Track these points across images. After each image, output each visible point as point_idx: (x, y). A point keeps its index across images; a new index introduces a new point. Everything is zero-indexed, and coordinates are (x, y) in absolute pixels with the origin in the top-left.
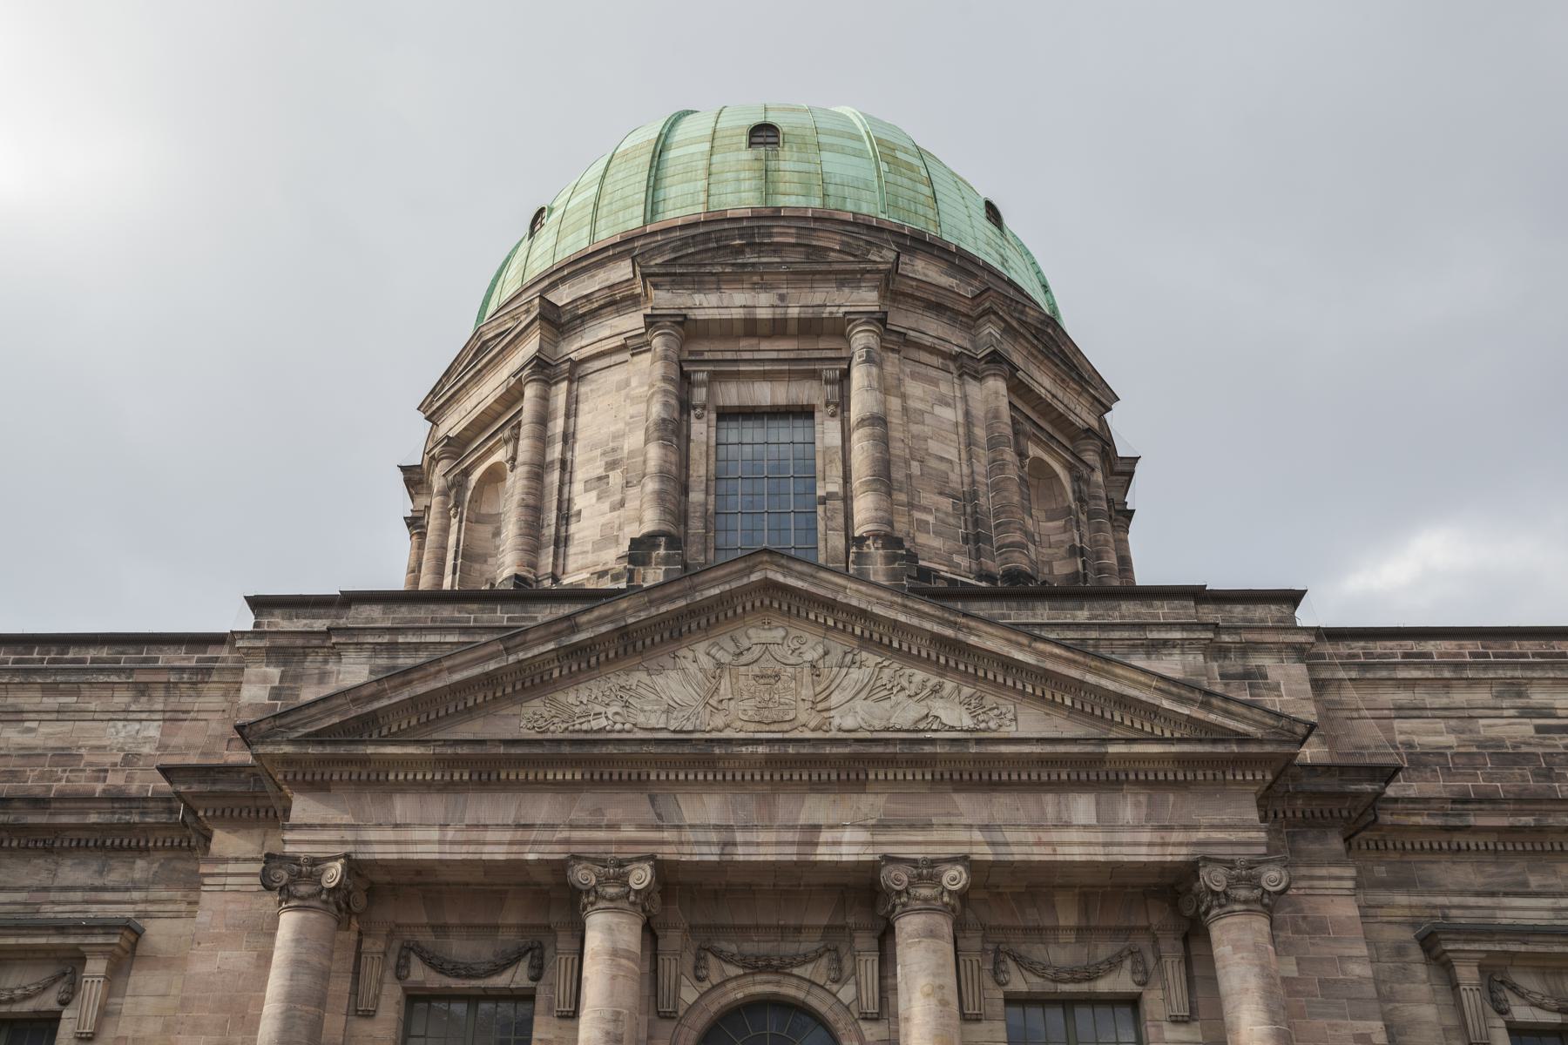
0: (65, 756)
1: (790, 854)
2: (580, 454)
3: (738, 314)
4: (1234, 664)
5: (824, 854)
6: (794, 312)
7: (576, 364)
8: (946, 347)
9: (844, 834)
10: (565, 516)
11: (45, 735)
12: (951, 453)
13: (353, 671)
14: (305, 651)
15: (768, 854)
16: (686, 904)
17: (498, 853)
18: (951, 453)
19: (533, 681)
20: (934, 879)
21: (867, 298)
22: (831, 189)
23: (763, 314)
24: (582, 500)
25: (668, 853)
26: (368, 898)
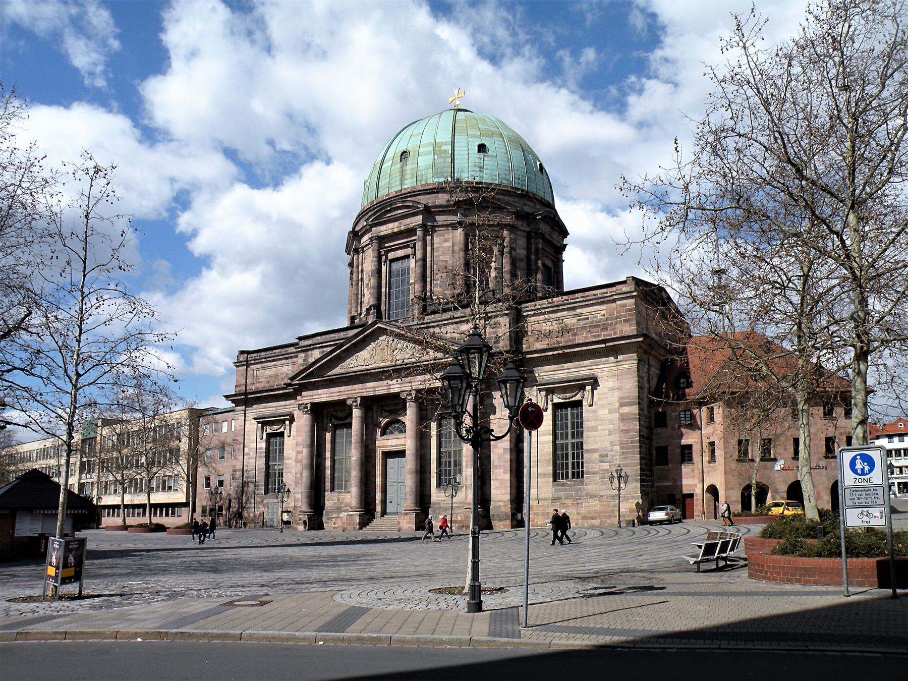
0: (276, 376)
1: (386, 392)
2: (365, 277)
3: (390, 232)
4: (492, 321)
5: (392, 391)
6: (403, 228)
7: (363, 248)
8: (445, 223)
9: (395, 386)
10: (363, 295)
11: (271, 372)
12: (447, 258)
13: (316, 354)
14: (307, 350)
15: (382, 392)
16: (370, 404)
17: (336, 398)
18: (447, 258)
19: (340, 359)
20: (411, 395)
21: (419, 219)
22: (419, 173)
23: (396, 230)
24: (366, 291)
25: (365, 394)
26: (318, 411)
